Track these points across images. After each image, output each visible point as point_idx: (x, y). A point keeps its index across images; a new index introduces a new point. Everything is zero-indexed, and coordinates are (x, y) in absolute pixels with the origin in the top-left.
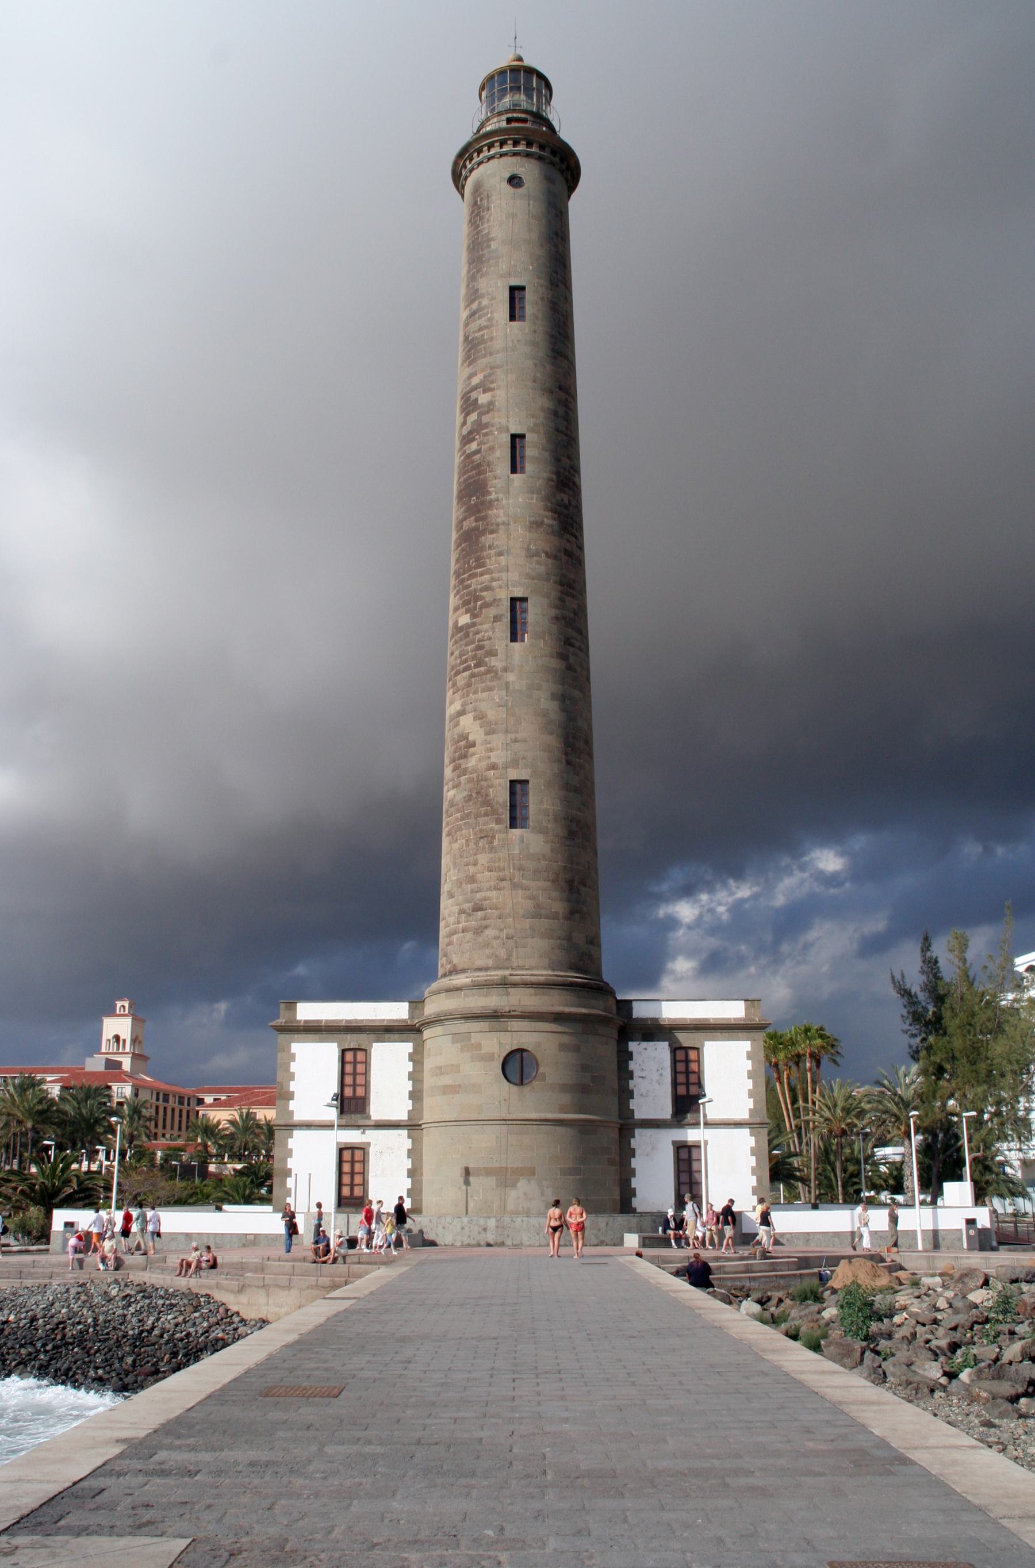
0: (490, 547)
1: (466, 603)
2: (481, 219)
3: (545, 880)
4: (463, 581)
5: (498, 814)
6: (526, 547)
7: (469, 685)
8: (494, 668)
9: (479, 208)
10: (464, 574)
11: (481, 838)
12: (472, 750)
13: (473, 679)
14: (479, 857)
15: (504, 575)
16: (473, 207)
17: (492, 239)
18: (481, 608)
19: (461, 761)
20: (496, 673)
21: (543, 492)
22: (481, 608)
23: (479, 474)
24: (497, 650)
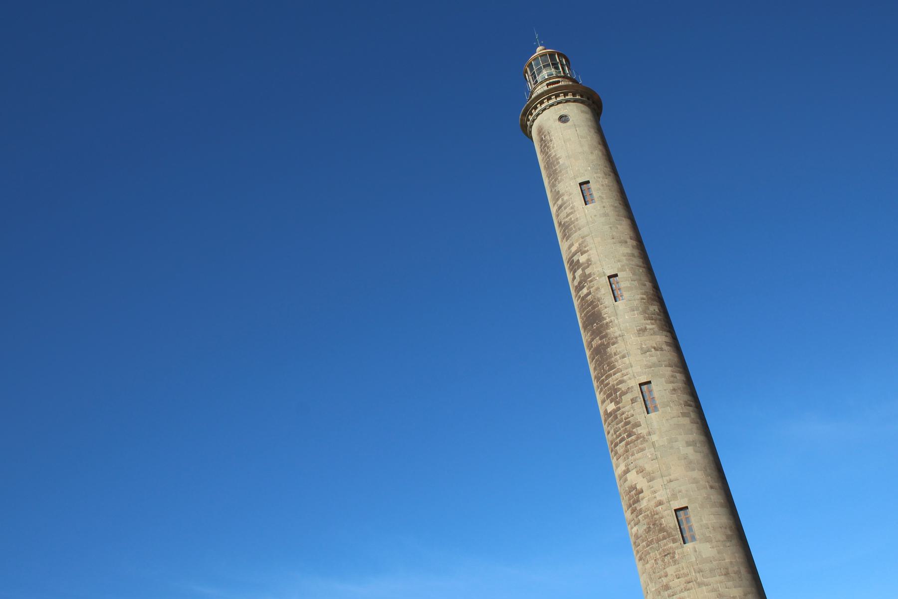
0: (615, 354)
1: (609, 396)
2: (548, 149)
3: (719, 576)
4: (602, 382)
5: (673, 536)
6: (639, 347)
7: (627, 451)
8: (641, 435)
9: (545, 141)
10: (602, 377)
11: (665, 555)
12: (641, 495)
13: (628, 446)
14: (667, 569)
15: (630, 370)
16: (540, 142)
17: (559, 158)
18: (621, 396)
19: (636, 505)
20: (643, 437)
21: (640, 308)
22: (621, 396)
23: (594, 308)
24: (640, 422)
